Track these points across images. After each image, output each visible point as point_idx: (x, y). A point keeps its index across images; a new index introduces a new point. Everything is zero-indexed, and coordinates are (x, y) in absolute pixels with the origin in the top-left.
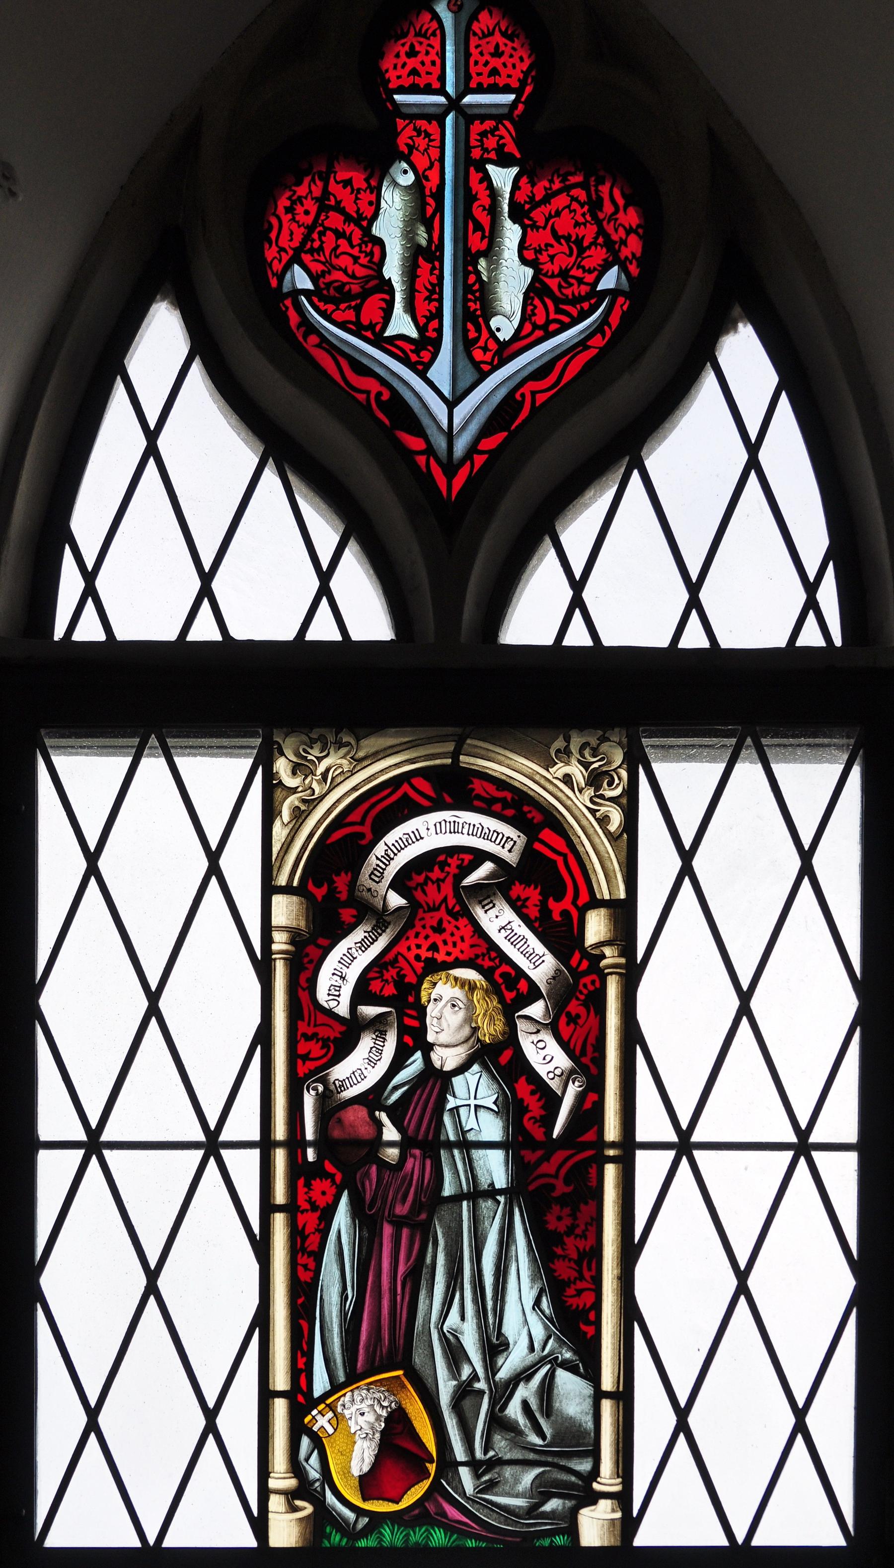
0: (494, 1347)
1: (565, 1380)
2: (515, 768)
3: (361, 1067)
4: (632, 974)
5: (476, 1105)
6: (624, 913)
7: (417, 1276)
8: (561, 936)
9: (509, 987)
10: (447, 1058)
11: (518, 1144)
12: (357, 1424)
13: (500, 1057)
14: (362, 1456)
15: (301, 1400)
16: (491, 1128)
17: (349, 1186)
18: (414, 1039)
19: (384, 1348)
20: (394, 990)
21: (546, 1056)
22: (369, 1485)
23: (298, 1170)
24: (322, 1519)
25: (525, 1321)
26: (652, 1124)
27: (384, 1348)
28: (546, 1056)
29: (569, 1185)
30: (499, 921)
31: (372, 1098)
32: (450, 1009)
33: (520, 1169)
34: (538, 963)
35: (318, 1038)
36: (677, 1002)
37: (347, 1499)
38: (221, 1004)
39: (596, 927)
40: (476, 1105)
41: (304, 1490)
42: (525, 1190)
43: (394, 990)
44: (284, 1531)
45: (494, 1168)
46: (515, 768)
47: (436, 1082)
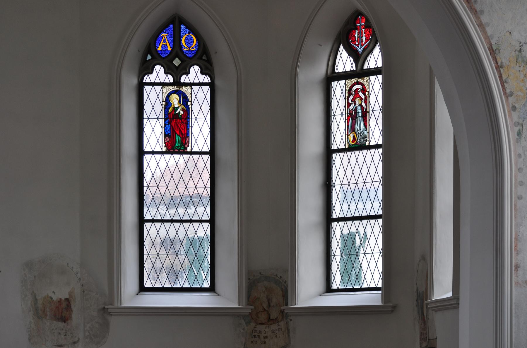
0: (360, 129)
1: (365, 132)
2: (360, 80)
3: (352, 107)
4: (369, 97)
5: (359, 109)
6: (369, 92)
7: (355, 124)
8: (364, 94)
9: (361, 99)
10: (357, 105)
11: (362, 112)
12: (351, 136)
13: (361, 105)
14: (352, 139)
15: (348, 135)
16: (360, 111)
17: (352, 117)
18: (355, 104)
19: (353, 130)
20: (354, 100)
21: (364, 104)
22: (352, 142)
23: (348, 116)
24: (349, 145)
25: (362, 127)
26: (371, 109)
27: (353, 130)
28: (364, 104)
29: (365, 114)
30: (361, 94)
31: (352, 110)
32: (357, 101)
33: (362, 114)
34: (363, 97)
35: (349, 105)
36: (372, 99)
37: (351, 143)
38: (342, 103)
39: (367, 93)
40: (359, 109)
41: (348, 143)
42: (363, 116)
43: (354, 100)
44: (347, 147)
45: (360, 114)
46: (360, 80)
47: (356, 107)
